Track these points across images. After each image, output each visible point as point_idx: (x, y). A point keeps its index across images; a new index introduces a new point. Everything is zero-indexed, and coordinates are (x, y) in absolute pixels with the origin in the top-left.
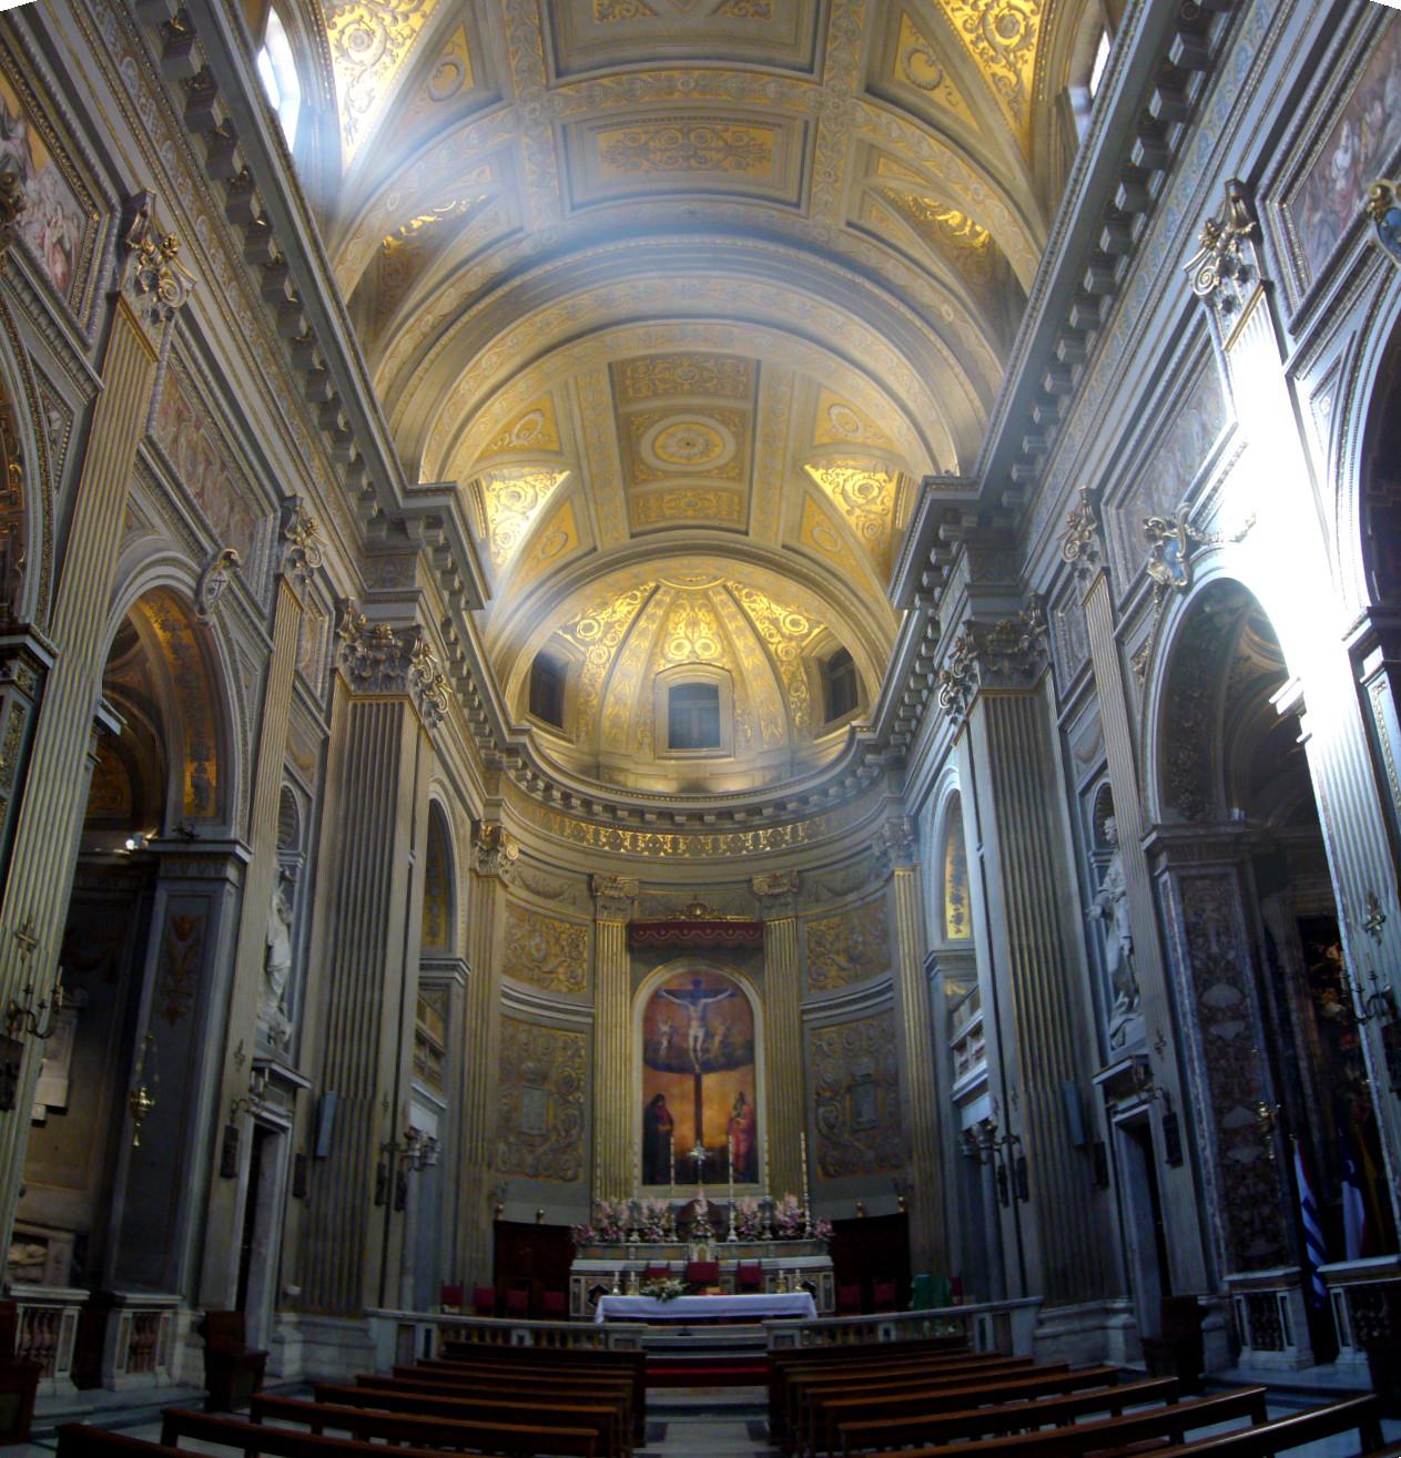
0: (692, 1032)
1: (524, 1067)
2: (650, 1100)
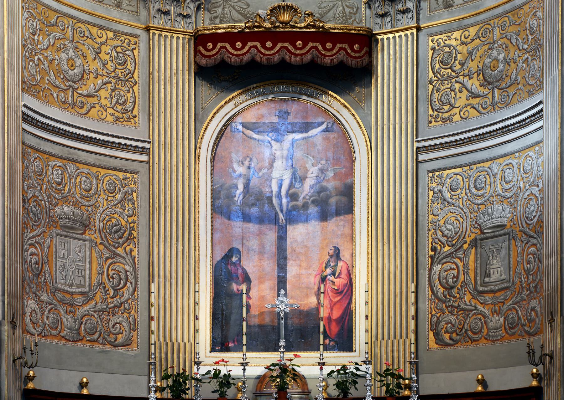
0: (276, 174)
1: (58, 210)
2: (218, 257)
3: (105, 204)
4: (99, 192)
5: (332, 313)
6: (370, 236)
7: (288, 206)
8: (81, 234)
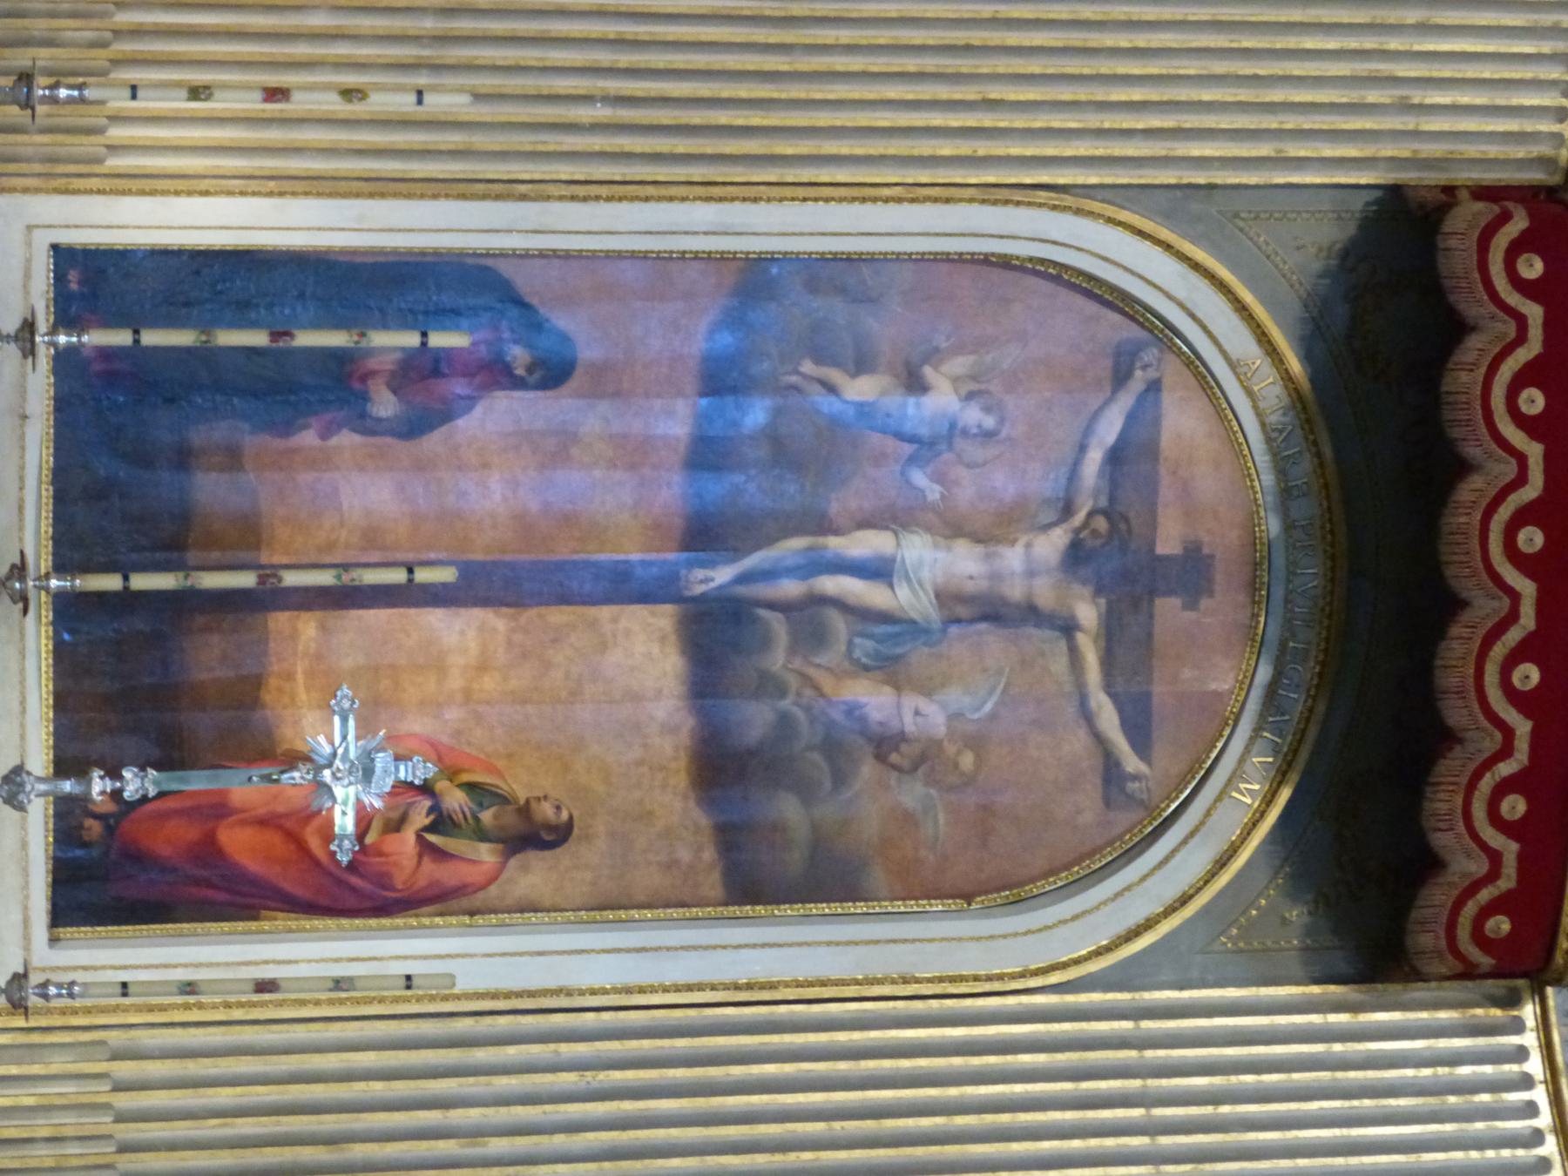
5: (244, 823)
7: (772, 605)
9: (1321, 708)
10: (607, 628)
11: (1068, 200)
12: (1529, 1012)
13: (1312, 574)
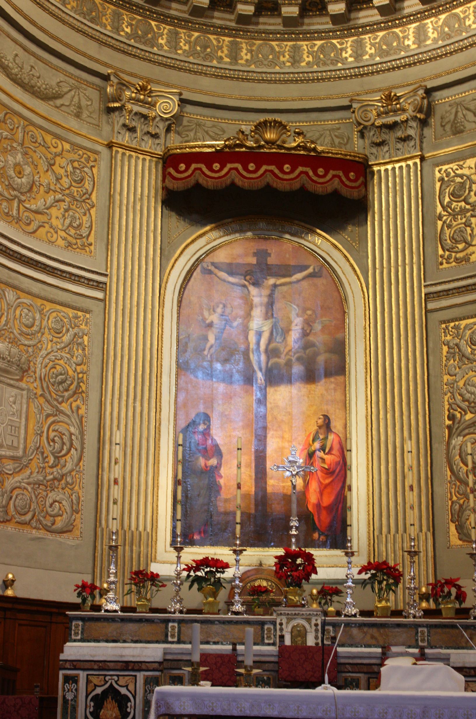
3: (49, 347)
4: (42, 330)
5: (322, 499)
6: (368, 401)
7: (267, 363)
8: (17, 380)
9: (296, 222)
10: (273, 405)
11: (163, 285)
12: (376, 169)
13: (262, 225)
